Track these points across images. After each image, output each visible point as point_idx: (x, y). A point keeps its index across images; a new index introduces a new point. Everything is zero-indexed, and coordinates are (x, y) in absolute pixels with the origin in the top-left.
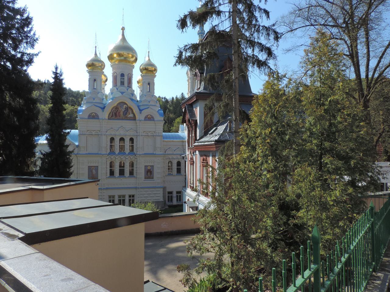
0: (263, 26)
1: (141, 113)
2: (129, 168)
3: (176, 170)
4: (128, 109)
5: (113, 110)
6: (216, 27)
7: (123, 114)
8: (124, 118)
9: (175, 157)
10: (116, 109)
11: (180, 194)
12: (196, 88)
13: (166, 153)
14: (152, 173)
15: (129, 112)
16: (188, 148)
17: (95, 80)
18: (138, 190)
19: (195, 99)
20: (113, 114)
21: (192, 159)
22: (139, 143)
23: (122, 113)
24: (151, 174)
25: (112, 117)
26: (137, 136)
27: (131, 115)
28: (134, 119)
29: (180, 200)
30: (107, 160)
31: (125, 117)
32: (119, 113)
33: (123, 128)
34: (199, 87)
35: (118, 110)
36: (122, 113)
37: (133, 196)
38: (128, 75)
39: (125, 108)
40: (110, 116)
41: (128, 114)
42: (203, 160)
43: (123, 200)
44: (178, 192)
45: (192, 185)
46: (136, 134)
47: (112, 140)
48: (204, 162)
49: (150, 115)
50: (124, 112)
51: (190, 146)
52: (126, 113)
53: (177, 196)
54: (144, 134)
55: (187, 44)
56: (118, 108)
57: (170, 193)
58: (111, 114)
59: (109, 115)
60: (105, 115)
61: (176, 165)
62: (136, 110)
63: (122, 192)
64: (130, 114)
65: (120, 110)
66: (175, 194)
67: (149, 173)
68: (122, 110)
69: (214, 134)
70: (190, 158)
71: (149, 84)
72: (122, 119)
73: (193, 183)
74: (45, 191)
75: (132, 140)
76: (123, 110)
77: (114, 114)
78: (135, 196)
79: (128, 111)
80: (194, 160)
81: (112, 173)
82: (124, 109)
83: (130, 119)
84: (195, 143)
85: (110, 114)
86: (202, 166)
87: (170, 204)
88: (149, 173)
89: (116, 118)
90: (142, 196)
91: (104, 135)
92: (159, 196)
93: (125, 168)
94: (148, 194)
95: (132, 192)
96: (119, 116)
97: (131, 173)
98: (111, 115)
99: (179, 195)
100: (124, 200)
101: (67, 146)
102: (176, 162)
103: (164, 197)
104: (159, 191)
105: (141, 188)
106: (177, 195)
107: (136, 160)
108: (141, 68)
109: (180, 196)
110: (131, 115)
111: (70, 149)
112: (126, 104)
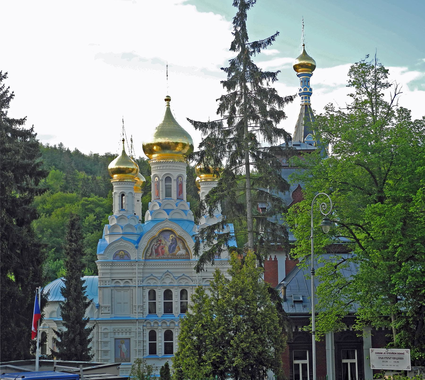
5: (153, 243)
8: (170, 256)
10: (157, 242)
17: (123, 195)
23: (166, 249)
27: (182, 252)
30: (145, 328)
31: (172, 255)
32: (163, 249)
35: (160, 244)
36: (166, 249)
38: (178, 178)
39: (172, 240)
40: (148, 255)
50: (170, 246)
52: (174, 248)
56: (161, 241)
58: (150, 250)
59: (146, 252)
65: (164, 243)
68: (167, 242)
72: (168, 258)
76: (169, 244)
77: (154, 250)
79: (176, 245)
82: (171, 242)
83: (181, 257)
85: (147, 251)
89: (158, 258)
96: (163, 254)
98: (149, 252)
110: (182, 252)
112: (171, 232)
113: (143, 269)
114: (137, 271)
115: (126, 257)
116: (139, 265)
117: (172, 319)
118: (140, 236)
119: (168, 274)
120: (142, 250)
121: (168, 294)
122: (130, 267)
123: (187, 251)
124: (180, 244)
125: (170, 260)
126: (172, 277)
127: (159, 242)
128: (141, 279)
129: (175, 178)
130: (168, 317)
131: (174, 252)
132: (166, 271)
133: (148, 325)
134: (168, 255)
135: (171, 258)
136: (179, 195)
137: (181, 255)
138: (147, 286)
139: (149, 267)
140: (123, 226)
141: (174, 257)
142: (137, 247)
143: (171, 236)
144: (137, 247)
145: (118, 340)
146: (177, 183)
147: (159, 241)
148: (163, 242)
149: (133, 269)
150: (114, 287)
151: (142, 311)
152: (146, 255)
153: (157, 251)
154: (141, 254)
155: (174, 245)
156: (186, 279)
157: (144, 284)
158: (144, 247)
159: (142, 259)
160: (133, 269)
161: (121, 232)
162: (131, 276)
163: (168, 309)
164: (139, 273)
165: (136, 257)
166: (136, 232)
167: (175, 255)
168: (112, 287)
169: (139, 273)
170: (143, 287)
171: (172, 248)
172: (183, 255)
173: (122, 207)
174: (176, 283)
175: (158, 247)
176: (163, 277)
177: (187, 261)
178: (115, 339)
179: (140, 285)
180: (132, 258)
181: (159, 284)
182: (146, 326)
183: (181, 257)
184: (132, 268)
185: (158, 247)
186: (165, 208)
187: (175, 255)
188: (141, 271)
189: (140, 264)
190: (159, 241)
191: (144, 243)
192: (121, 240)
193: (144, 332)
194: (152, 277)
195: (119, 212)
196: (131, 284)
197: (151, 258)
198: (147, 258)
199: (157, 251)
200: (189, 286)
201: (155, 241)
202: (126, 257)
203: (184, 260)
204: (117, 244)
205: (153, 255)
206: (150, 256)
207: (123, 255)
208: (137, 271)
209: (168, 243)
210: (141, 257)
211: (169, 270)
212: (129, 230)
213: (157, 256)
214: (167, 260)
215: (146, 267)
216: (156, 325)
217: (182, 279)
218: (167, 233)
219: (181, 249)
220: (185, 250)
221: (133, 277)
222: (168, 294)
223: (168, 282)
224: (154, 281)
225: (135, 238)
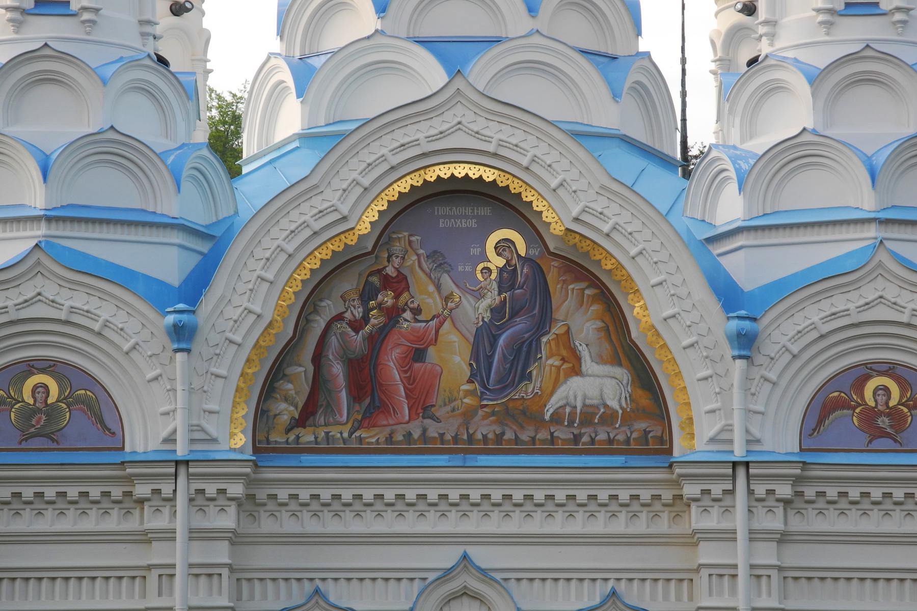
1: (746, 344)
5: (330, 308)
8: (484, 428)
10: (367, 294)
15: (566, 337)
23: (453, 358)
25: (306, 417)
27: (599, 384)
28: (645, 424)
31: (507, 415)
32: (419, 355)
35: (393, 314)
36: (453, 358)
40: (285, 411)
41: (548, 361)
49: (891, 370)
52: (524, 354)
56: (399, 284)
58: (301, 371)
59: (269, 391)
62: (671, 308)
64: (576, 371)
65: (431, 303)
68: (459, 300)
72: (466, 446)
76: (476, 310)
77: (337, 370)
79: (544, 320)
82: (492, 298)
83: (586, 433)
85: (276, 373)
89: (371, 436)
96: (422, 406)
98: (297, 385)
110: (599, 384)
113: (235, 539)
114: (179, 554)
115: (76, 425)
116: (198, 499)
118: (211, 247)
122: (112, 523)
123: (644, 378)
125: (483, 460)
127: (387, 298)
131: (528, 389)
134: (468, 415)
135: (497, 445)
139: (289, 525)
140: (53, 146)
142: (182, 335)
144: (182, 335)
147: (387, 282)
148: (425, 295)
149: (145, 538)
152: (262, 416)
155: (521, 325)
158: (247, 335)
160: (145, 538)
161: (36, 198)
164: (202, 572)
165: (179, 422)
166: (171, 206)
167: (538, 421)
169: (202, 572)
172: (609, 417)
175: (377, 341)
177: (661, 460)
180: (142, 436)
183: (586, 433)
184: (132, 524)
185: (377, 341)
186: (428, 30)
187: (529, 415)
188: (221, 553)
189: (211, 489)
190: (387, 282)
192: (37, 270)
195: (18, 25)
197: (307, 437)
198: (278, 438)
199: (365, 379)
201: (349, 284)
203: (619, 460)
205: (331, 409)
207: (52, 412)
209: (468, 303)
211: (482, 556)
212: (111, 190)
213: (367, 420)
214: (457, 460)
215: (267, 525)
218: (455, 217)
219: (588, 364)
220: (623, 374)
225: (167, 262)
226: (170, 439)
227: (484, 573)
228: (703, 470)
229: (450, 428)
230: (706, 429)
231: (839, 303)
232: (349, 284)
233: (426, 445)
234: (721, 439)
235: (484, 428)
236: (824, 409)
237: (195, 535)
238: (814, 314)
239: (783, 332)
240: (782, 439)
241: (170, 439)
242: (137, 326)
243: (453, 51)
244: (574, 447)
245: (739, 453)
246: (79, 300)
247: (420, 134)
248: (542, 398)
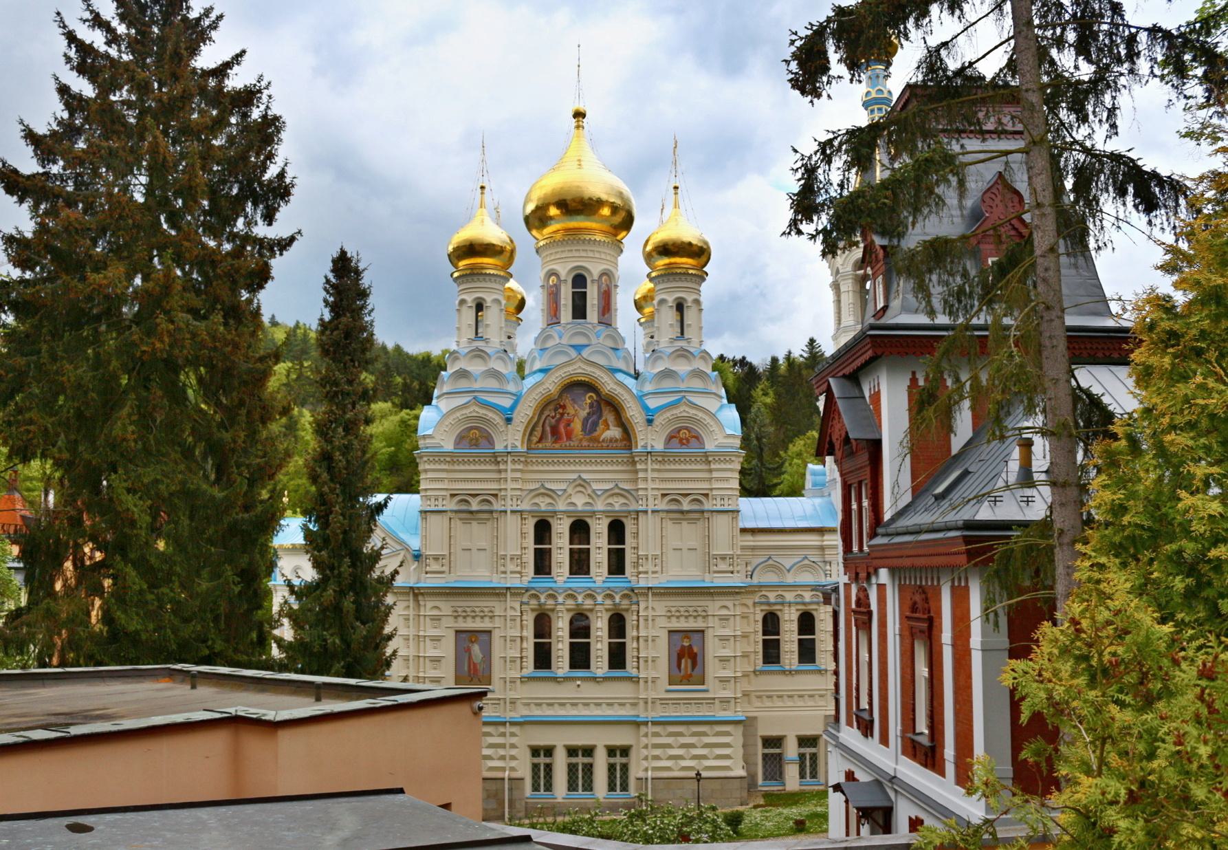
0: (1154, 31)
1: (650, 422)
2: (606, 640)
3: (795, 647)
4: (599, 405)
5: (546, 413)
6: (943, 53)
7: (584, 429)
8: (585, 443)
9: (789, 596)
10: (555, 410)
11: (813, 750)
12: (870, 311)
13: (755, 581)
14: (699, 659)
15: (606, 421)
16: (845, 559)
18: (643, 729)
19: (869, 354)
20: (543, 431)
21: (863, 601)
22: (645, 539)
23: (577, 426)
24: (694, 665)
25: (540, 440)
26: (637, 512)
27: (614, 432)
29: (814, 775)
31: (591, 440)
33: (581, 485)
34: (880, 305)
35: (562, 415)
36: (577, 426)
37: (625, 751)
39: (591, 406)
40: (535, 439)
41: (601, 427)
42: (914, 609)
43: (585, 765)
44: (804, 741)
45: (866, 716)
46: (633, 507)
47: (543, 530)
48: (917, 615)
49: (686, 428)
50: (585, 421)
51: (855, 549)
52: (595, 424)
53: (802, 757)
54: (663, 505)
55: (831, 136)
56: (564, 407)
57: (773, 742)
58: (539, 429)
59: (531, 434)
60: (511, 438)
61: (795, 626)
63: (580, 738)
65: (572, 411)
66: (791, 750)
67: (687, 657)
68: (579, 411)
69: (956, 496)
70: (854, 598)
71: (680, 307)
72: (582, 448)
73: (871, 704)
74: (284, 735)
75: (617, 530)
76: (584, 413)
77: (548, 429)
78: (633, 753)
79: (600, 417)
80: (874, 607)
81: (543, 658)
82: (587, 410)
84: (873, 535)
85: (533, 429)
86: (907, 633)
87: (774, 787)
88: (687, 657)
89: (557, 446)
90: (657, 752)
91: (512, 512)
92: (728, 757)
93: (592, 640)
94: (683, 746)
95: (620, 737)
96: (569, 436)
97: (617, 658)
98: (538, 433)
99: (808, 751)
100: (591, 765)
101: (376, 556)
102: (795, 616)
103: (748, 762)
104: (728, 734)
105: (655, 723)
106: (803, 750)
107: (634, 607)
108: (649, 248)
109: (814, 757)
111: (386, 566)
115: (483, 442)
117: (590, 589)
118: (518, 398)
119: (580, 485)
120: (521, 428)
121: (580, 529)
124: (609, 417)
126: (589, 492)
128: (519, 493)
129: (596, 277)
130: (580, 583)
131: (596, 434)
132: (575, 476)
133: (534, 602)
135: (588, 448)
136: (603, 315)
137: (611, 441)
138: (530, 512)
139: (535, 468)
141: (595, 443)
143: (589, 398)
145: (464, 635)
146: (599, 288)
148: (570, 410)
149: (500, 471)
150: (456, 512)
151: (519, 569)
152: (529, 440)
153: (555, 431)
154: (519, 436)
155: (594, 417)
156: (622, 495)
157: (525, 506)
158: (525, 420)
159: (521, 448)
160: (500, 471)
162: (495, 486)
163: (580, 564)
168: (452, 511)
170: (521, 512)
171: (590, 426)
172: (616, 441)
173: (477, 333)
174: (600, 506)
175: (558, 421)
176: (570, 491)
178: (457, 632)
179: (515, 508)
181: (561, 506)
182: (527, 604)
183: (611, 444)
185: (558, 421)
187: (596, 440)
191: (524, 414)
193: (524, 617)
194: (543, 491)
196: (497, 506)
197: (540, 446)
199: (555, 431)
200: (629, 512)
201: (551, 407)
202: (483, 442)
204: (464, 412)
206: (540, 440)
207: (477, 440)
208: (510, 475)
210: (518, 444)
211: (584, 476)
213: (555, 442)
215: (530, 468)
216: (551, 602)
217: (612, 495)
220: (620, 430)
221: (500, 490)
222: (580, 529)
223: (580, 502)
224: (549, 500)
226: (506, 447)
227: (584, 480)
228: (640, 454)
229: (576, 443)
230: (641, 443)
231: (675, 412)
232: (551, 407)
233: (571, 448)
234: (645, 447)
235: (585, 443)
236: (670, 438)
237: (513, 470)
238: (668, 414)
239: (659, 420)
240: (659, 446)
241: (506, 447)
242: (498, 419)
243: (578, 348)
244: (608, 448)
245: (649, 449)
246: (484, 412)
247: (570, 369)
248: (600, 436)
